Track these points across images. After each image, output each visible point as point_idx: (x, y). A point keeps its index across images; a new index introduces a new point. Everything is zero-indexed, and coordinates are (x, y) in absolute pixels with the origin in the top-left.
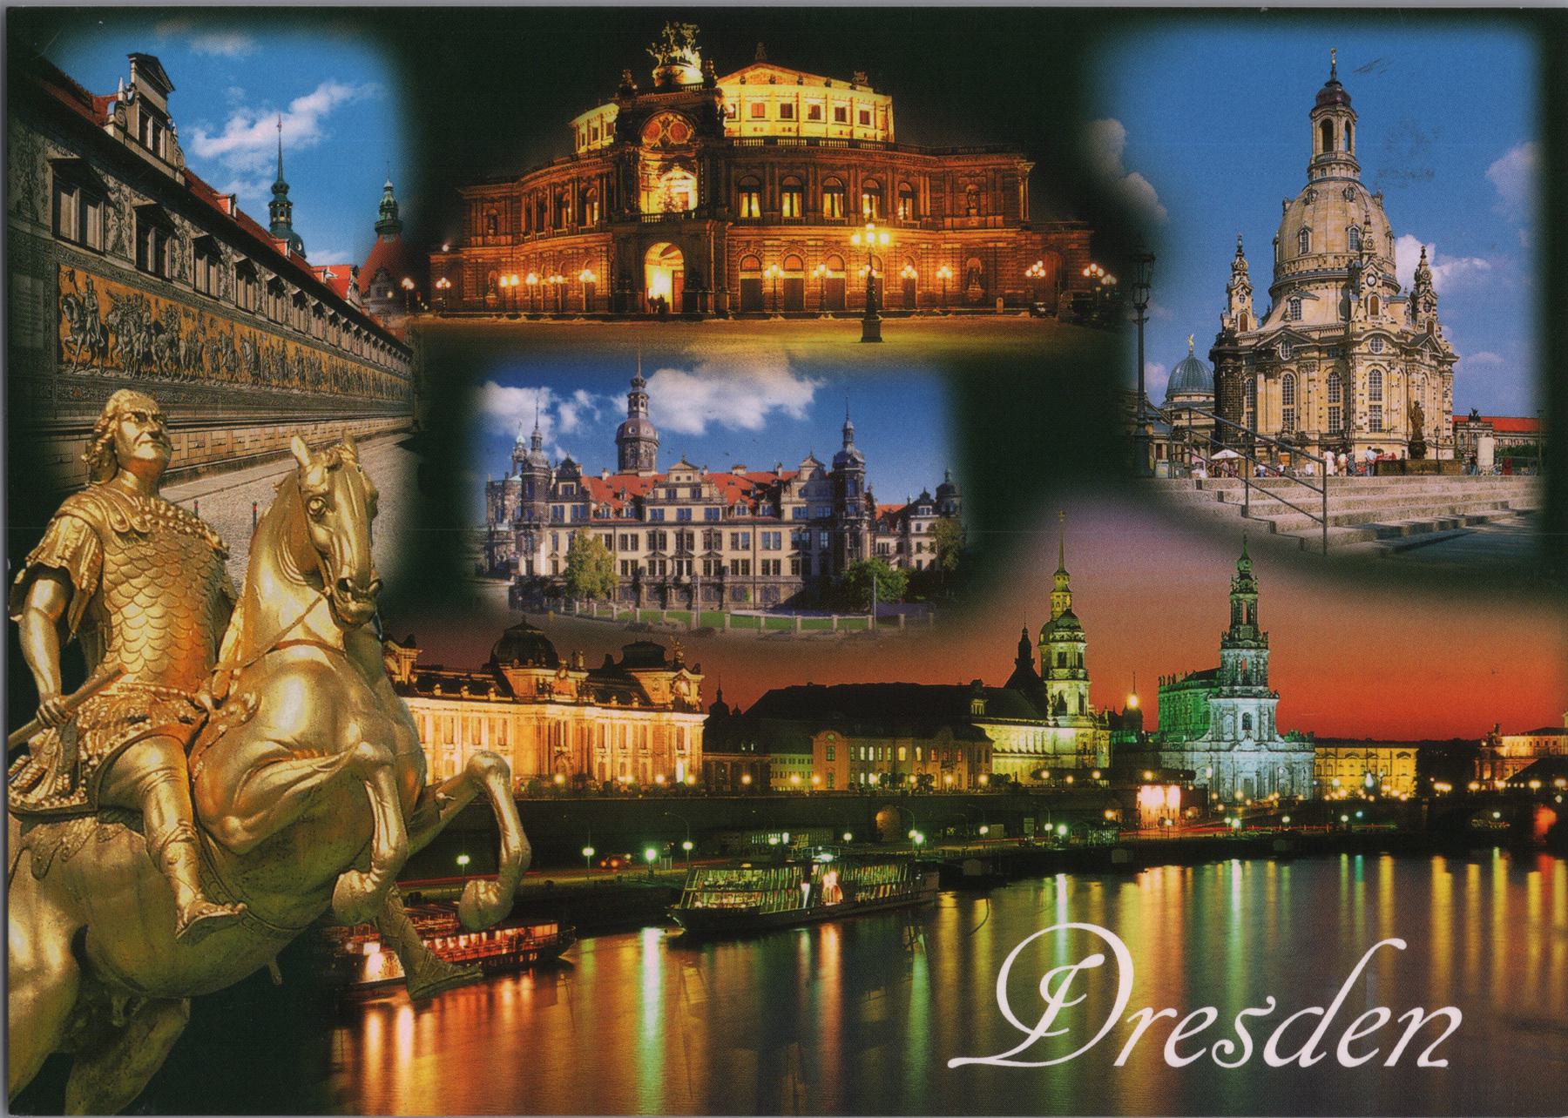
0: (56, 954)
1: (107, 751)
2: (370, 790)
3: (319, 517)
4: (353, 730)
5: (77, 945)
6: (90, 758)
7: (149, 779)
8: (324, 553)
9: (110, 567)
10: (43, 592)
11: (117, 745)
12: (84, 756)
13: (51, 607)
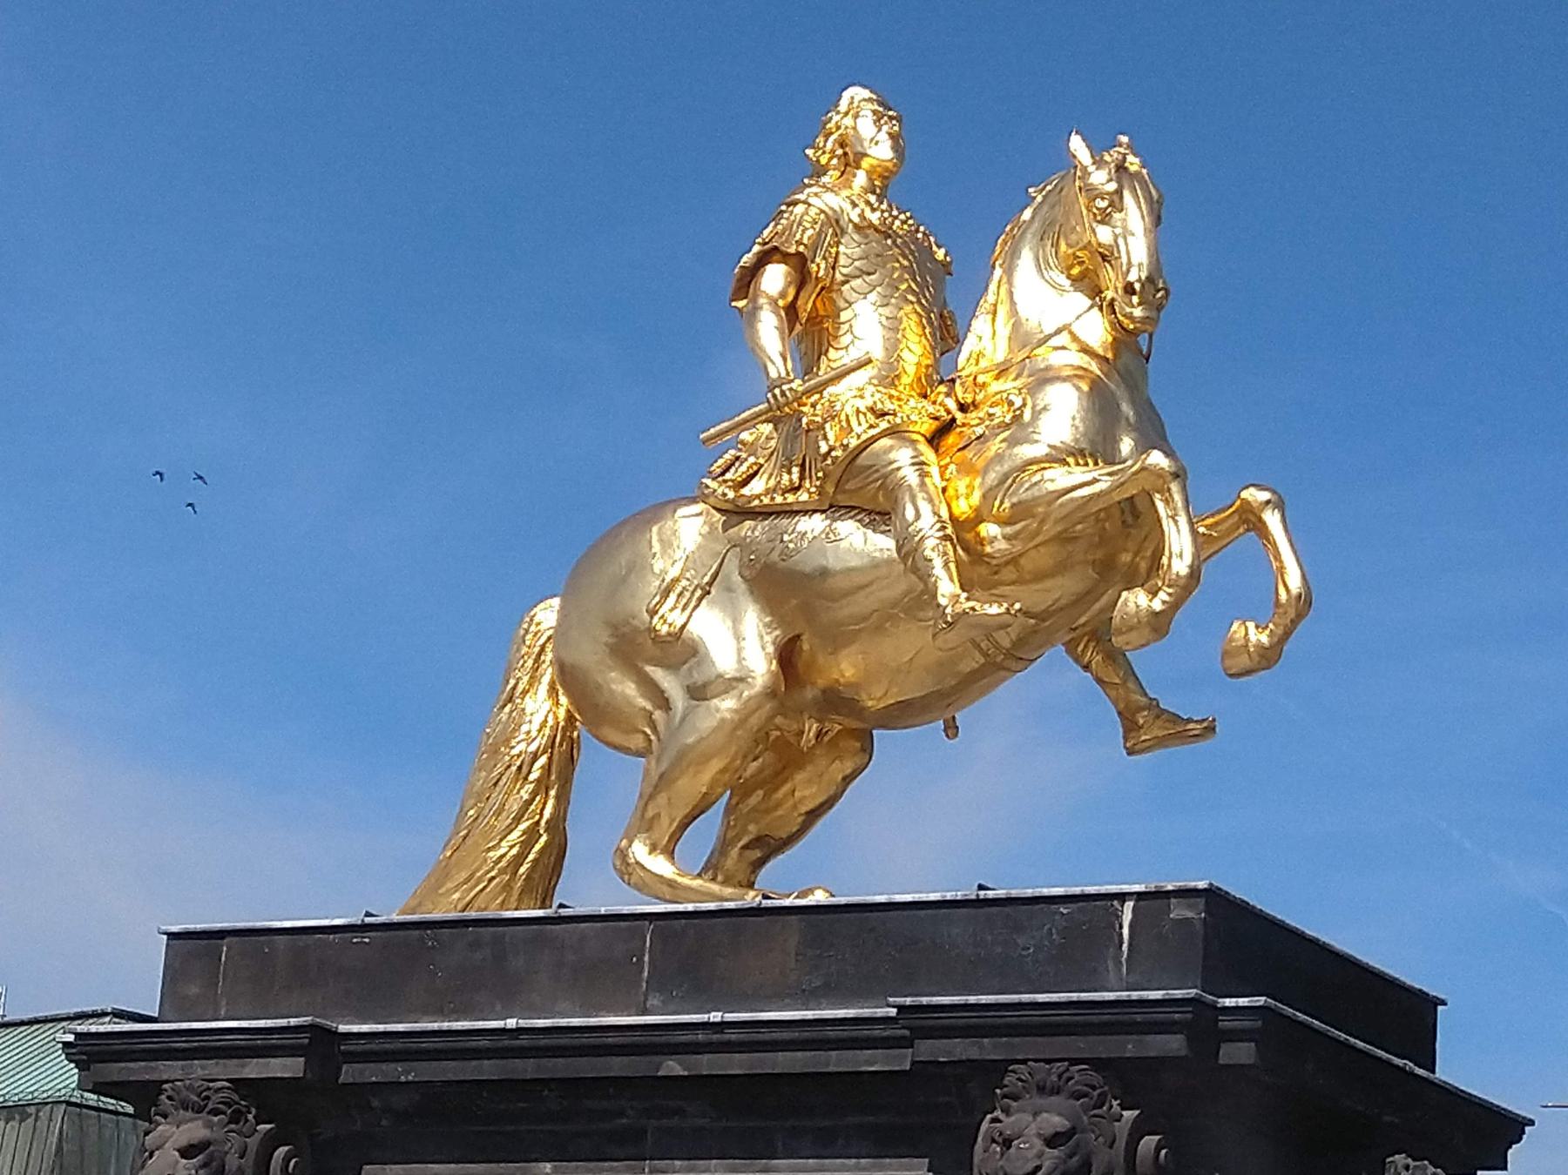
0: (760, 665)
1: (854, 442)
2: (1160, 505)
3: (1105, 219)
4: (1126, 445)
5: (787, 656)
6: (832, 449)
7: (901, 474)
8: (1106, 256)
9: (842, 260)
10: (775, 278)
11: (864, 437)
12: (824, 448)
13: (783, 295)
